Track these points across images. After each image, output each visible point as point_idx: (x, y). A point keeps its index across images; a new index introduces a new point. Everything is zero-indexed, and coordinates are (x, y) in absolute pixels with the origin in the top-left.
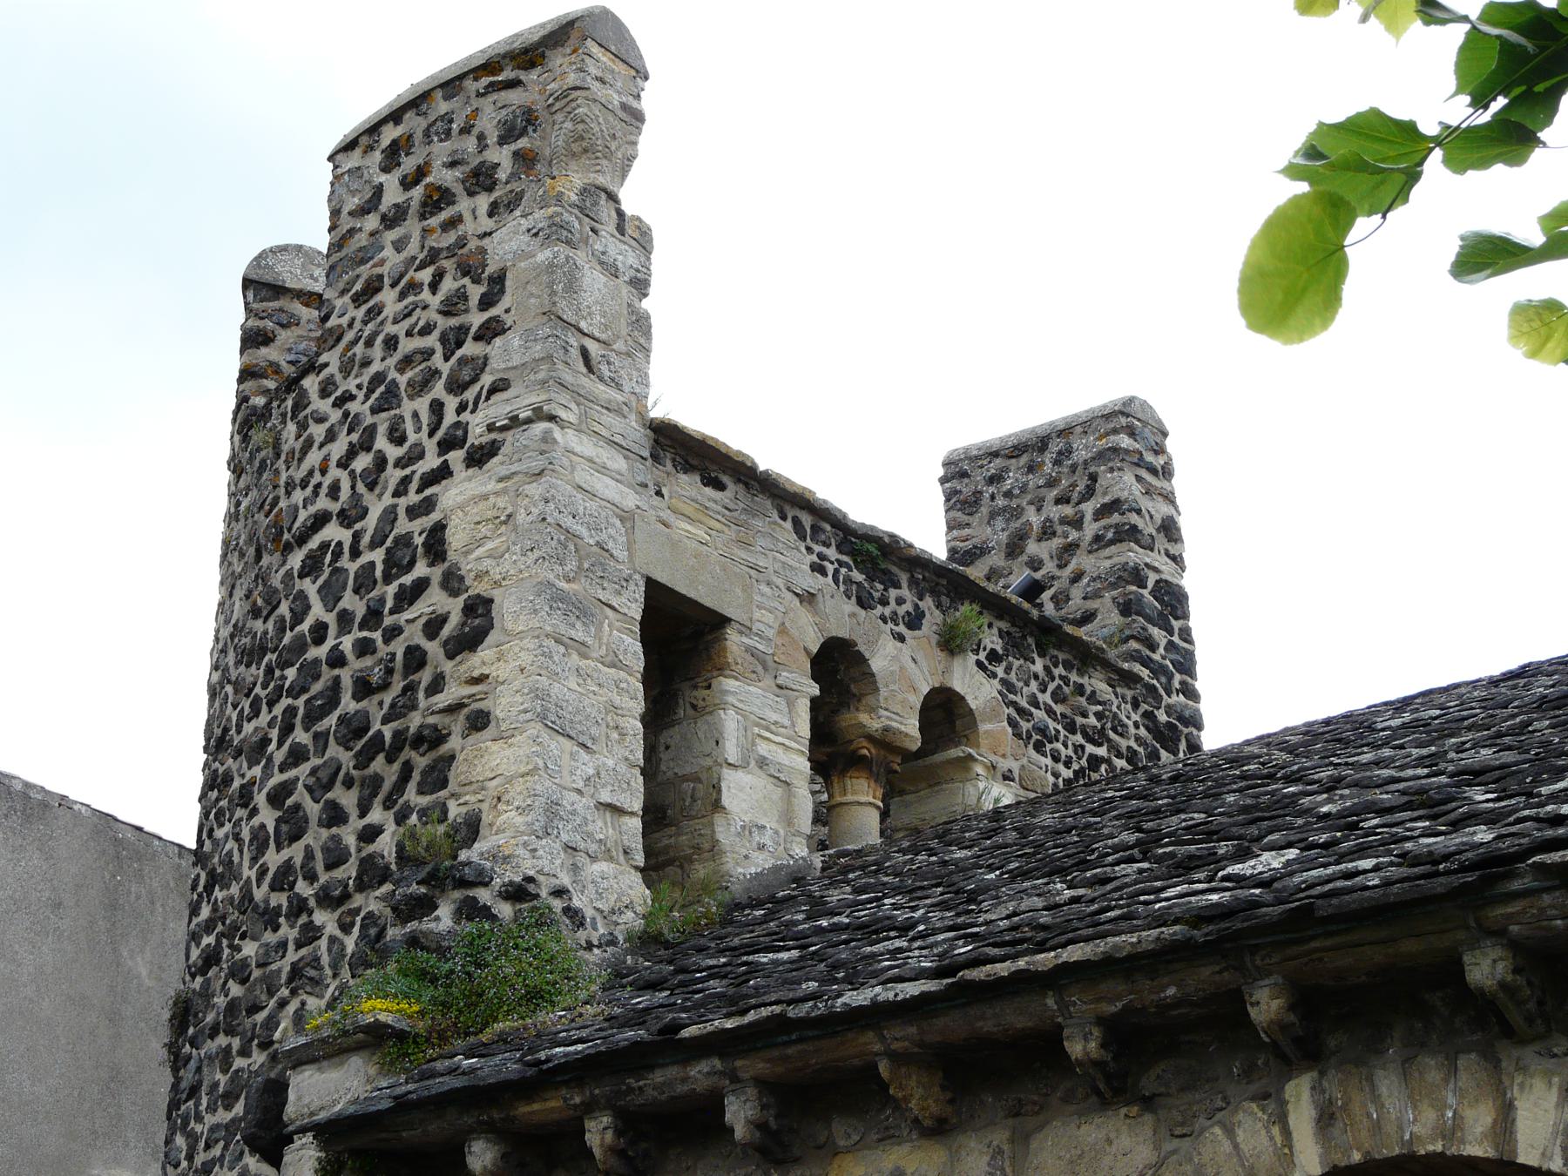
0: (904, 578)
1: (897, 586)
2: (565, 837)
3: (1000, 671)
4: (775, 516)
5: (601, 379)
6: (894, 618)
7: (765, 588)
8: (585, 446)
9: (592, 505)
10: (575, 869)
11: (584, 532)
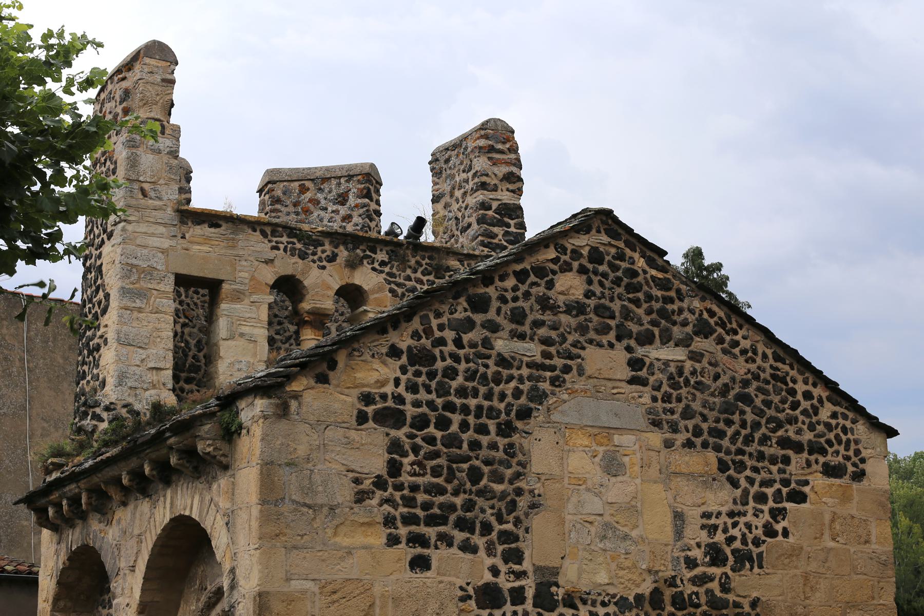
0: (327, 242)
1: (323, 245)
2: (129, 384)
3: (387, 269)
4: (250, 231)
5: (151, 198)
6: (320, 259)
7: (244, 263)
8: (143, 228)
9: (145, 251)
10: (136, 395)
11: (140, 263)
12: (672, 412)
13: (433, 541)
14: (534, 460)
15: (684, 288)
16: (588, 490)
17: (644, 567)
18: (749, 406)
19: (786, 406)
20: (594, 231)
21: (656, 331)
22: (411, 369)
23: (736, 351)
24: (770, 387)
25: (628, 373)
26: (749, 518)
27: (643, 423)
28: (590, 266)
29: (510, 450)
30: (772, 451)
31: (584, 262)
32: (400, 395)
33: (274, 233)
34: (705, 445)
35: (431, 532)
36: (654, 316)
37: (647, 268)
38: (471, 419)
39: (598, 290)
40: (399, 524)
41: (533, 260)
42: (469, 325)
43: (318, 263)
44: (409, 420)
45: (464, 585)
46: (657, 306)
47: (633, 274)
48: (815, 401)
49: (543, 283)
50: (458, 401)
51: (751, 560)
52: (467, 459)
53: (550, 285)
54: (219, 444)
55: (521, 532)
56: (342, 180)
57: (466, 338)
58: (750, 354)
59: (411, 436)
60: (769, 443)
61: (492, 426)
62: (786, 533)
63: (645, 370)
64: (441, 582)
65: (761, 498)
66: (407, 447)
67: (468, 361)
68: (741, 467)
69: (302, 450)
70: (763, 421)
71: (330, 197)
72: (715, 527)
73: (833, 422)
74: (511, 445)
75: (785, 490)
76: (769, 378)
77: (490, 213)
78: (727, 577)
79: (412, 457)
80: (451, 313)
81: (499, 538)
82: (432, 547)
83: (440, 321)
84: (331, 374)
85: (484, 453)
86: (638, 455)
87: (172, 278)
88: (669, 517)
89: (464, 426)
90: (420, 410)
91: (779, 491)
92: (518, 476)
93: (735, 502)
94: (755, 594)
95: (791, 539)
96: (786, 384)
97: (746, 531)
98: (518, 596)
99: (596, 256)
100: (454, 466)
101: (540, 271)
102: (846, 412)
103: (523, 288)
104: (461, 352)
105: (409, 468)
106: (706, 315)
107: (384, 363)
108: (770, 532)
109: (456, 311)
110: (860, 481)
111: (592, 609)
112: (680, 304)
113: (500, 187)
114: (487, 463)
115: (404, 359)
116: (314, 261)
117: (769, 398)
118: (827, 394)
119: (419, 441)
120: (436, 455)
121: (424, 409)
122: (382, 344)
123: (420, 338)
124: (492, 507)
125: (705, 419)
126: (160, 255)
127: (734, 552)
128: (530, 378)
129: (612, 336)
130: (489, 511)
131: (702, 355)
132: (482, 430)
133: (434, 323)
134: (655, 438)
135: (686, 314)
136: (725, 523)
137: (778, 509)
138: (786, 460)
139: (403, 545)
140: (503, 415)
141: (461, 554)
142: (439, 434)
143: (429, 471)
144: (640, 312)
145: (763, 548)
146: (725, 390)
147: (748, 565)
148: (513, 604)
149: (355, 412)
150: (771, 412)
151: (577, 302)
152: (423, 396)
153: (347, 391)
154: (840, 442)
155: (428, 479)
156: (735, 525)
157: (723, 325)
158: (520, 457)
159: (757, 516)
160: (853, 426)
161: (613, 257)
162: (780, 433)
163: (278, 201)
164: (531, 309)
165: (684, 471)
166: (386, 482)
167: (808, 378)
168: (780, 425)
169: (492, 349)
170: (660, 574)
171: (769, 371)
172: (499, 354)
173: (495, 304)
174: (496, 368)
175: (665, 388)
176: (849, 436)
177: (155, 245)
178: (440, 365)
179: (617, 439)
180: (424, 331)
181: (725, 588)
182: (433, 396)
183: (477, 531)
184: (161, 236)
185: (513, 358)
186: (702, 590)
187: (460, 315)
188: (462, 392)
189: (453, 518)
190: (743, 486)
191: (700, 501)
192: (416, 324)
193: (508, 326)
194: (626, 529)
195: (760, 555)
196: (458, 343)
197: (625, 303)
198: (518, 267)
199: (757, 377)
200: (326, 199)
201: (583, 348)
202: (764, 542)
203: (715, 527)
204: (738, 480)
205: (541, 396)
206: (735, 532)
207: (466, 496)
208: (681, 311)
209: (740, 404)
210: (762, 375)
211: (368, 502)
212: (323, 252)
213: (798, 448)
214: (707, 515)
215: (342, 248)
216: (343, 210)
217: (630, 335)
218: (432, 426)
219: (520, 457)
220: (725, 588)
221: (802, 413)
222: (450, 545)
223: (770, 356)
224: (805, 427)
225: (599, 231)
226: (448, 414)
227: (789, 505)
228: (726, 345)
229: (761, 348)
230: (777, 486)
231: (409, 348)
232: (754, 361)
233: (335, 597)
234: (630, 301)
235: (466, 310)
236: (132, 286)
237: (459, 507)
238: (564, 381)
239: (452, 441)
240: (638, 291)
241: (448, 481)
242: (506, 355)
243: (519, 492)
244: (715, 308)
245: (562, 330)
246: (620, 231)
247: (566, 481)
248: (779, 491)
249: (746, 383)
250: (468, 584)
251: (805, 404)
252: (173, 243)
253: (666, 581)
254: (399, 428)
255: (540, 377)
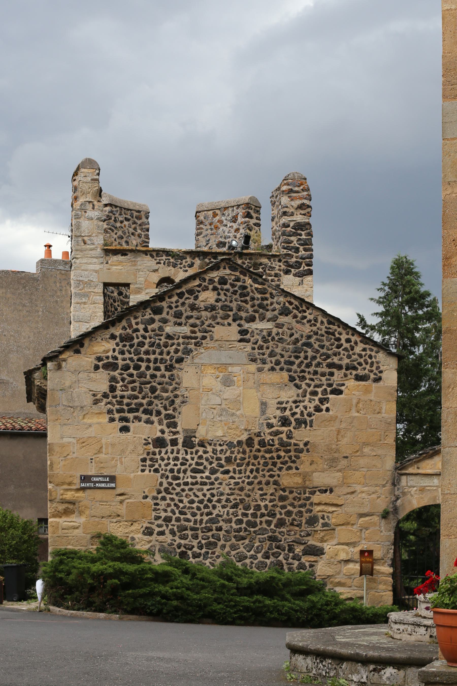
1: (186, 258)
4: (144, 256)
12: (263, 354)
13: (131, 420)
14: (184, 381)
15: (274, 292)
16: (213, 394)
17: (243, 428)
18: (310, 348)
19: (333, 347)
20: (222, 269)
21: (257, 315)
22: (121, 344)
23: (305, 321)
24: (324, 338)
25: (239, 337)
26: (306, 403)
27: (246, 360)
28: (219, 287)
29: (172, 378)
30: (323, 370)
31: (216, 284)
32: (115, 356)
33: (157, 255)
34: (282, 369)
35: (131, 416)
36: (256, 308)
37: (253, 284)
38: (151, 365)
39: (223, 297)
40: (115, 412)
41: (186, 287)
42: (152, 321)
43: (183, 268)
44: (120, 367)
45: (147, 438)
46: (257, 302)
47: (245, 288)
48: (352, 343)
49: (192, 297)
50: (145, 357)
51: (305, 423)
52: (149, 383)
53: (196, 298)
54: (42, 381)
55: (176, 414)
56: (235, 208)
57: (149, 327)
58: (313, 322)
59: (121, 374)
60: (321, 366)
61: (162, 367)
62: (328, 410)
63: (249, 335)
64: (135, 437)
65: (314, 393)
66: (119, 379)
67: (150, 338)
68: (304, 378)
69: (67, 384)
70: (318, 356)
71: (229, 218)
72: (285, 409)
73: (363, 353)
74: (172, 375)
75: (329, 389)
76: (324, 333)
77: (289, 229)
78: (290, 431)
79: (121, 383)
80: (143, 316)
81: (165, 417)
82: (131, 422)
83: (137, 321)
84: (82, 349)
85: (158, 379)
86: (242, 376)
87: (102, 285)
88: (258, 404)
89: (148, 368)
90: (125, 362)
91: (325, 389)
92: (175, 389)
93: (298, 395)
94: (306, 440)
95: (331, 413)
96: (334, 336)
97: (304, 410)
98: (174, 442)
99: (223, 281)
100: (143, 386)
101: (191, 292)
102: (372, 347)
103: (181, 301)
104: (147, 334)
105: (120, 388)
106: (287, 304)
107: (108, 342)
108: (318, 409)
109: (145, 315)
110: (378, 382)
111: (214, 447)
112: (272, 300)
113: (295, 213)
114: (159, 384)
115: (118, 340)
116: (181, 268)
117: (323, 344)
118: (360, 339)
119: (125, 376)
120: (134, 382)
121: (128, 362)
122: (107, 334)
123: (126, 329)
124: (162, 404)
125: (282, 356)
126: (94, 273)
127: (295, 420)
128: (183, 344)
129: (230, 320)
130: (160, 405)
131: (283, 325)
132: (157, 369)
133: (133, 322)
134: (253, 367)
135: (275, 305)
136: (291, 406)
137: (323, 398)
138: (332, 374)
139: (117, 422)
140: (169, 362)
141: (145, 424)
142: (135, 372)
143: (130, 389)
144: (248, 306)
145: (313, 417)
146: (297, 340)
147: (303, 426)
148: (172, 446)
149: (93, 365)
150: (325, 351)
151: (211, 305)
152: (127, 355)
153: (90, 356)
154: (367, 363)
155: (130, 392)
156: (297, 407)
157: (297, 308)
158: (177, 380)
159: (311, 402)
160: (376, 354)
161: (233, 280)
162: (329, 360)
163: (202, 223)
164: (186, 311)
165: (268, 382)
166: (109, 395)
167: (348, 332)
168: (328, 357)
169: (164, 331)
170: (252, 431)
171: (324, 329)
172: (167, 334)
173: (166, 310)
174: (165, 340)
175: (260, 342)
176: (373, 359)
177: (91, 269)
178: (136, 341)
179: (230, 369)
180: (128, 326)
181: (289, 437)
182: (132, 355)
183: (154, 414)
184: (95, 263)
185: (174, 335)
186: (276, 438)
187: (147, 317)
188: (147, 353)
189: (142, 409)
190: (303, 388)
191: (277, 396)
192: (124, 323)
193: (173, 320)
194: (234, 411)
195: (311, 421)
196: (146, 330)
197: (239, 303)
198: (178, 291)
199: (316, 334)
200: (226, 220)
201: (214, 327)
202: (314, 414)
203: (285, 409)
204: (301, 385)
205: (189, 352)
206: (298, 410)
207: (149, 399)
208: (272, 304)
209: (305, 347)
210: (320, 332)
211: (100, 404)
212: (186, 262)
213: (339, 367)
214: (279, 403)
215: (197, 259)
216: (235, 226)
217: (241, 318)
218: (132, 369)
219: (177, 380)
220: (289, 437)
221: (343, 350)
222: (140, 421)
223: (325, 322)
224: (345, 357)
225: (225, 268)
226: (140, 363)
227: (330, 396)
228: (298, 319)
229: (320, 318)
230: (324, 387)
231: (121, 335)
232: (315, 325)
233: (84, 444)
234: (242, 301)
235: (150, 314)
236: (80, 291)
237: (145, 404)
238: (202, 343)
239: (141, 375)
240: (246, 296)
241: (140, 393)
242: (171, 334)
243: (176, 396)
244: (292, 300)
245: (202, 319)
246: (237, 267)
247: (201, 390)
248: (325, 389)
249: (309, 337)
250: (149, 438)
251: (346, 345)
252: (101, 266)
253: (255, 434)
254: (115, 371)
255: (189, 342)
